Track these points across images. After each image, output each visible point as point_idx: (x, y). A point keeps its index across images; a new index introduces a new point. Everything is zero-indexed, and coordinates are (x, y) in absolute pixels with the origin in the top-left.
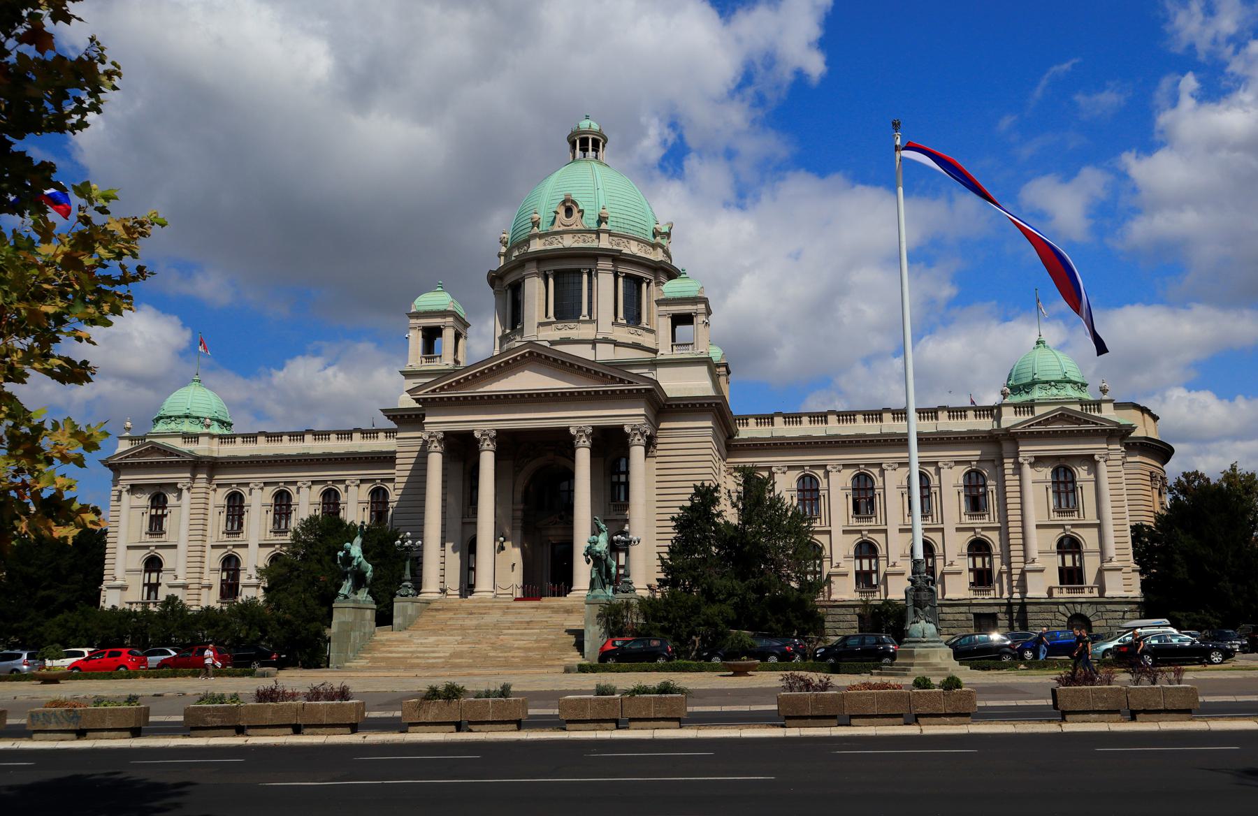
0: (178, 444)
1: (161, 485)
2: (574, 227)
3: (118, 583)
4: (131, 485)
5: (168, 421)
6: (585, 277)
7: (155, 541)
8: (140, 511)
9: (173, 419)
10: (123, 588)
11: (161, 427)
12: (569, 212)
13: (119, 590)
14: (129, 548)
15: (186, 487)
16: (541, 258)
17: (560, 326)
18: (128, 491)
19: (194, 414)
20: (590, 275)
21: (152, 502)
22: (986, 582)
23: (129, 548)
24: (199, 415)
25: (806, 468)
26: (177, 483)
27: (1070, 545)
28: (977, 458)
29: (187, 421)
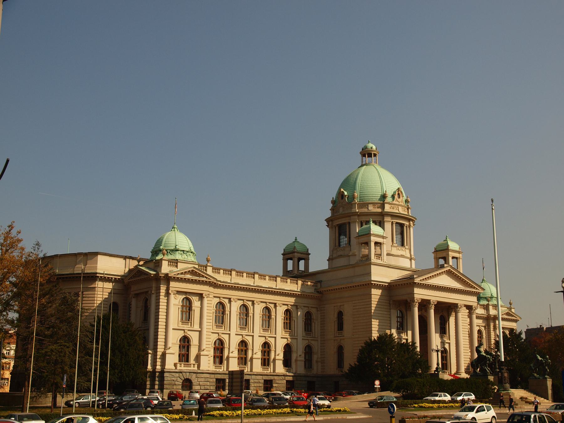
2: (401, 203)
4: (177, 291)
5: (182, 252)
6: (405, 227)
7: (186, 327)
9: (185, 252)
12: (399, 194)
14: (173, 329)
16: (393, 216)
17: (400, 248)
20: (406, 226)
22: (267, 364)
23: (173, 329)
25: (289, 305)
26: (202, 294)
27: (185, 342)
28: (292, 304)
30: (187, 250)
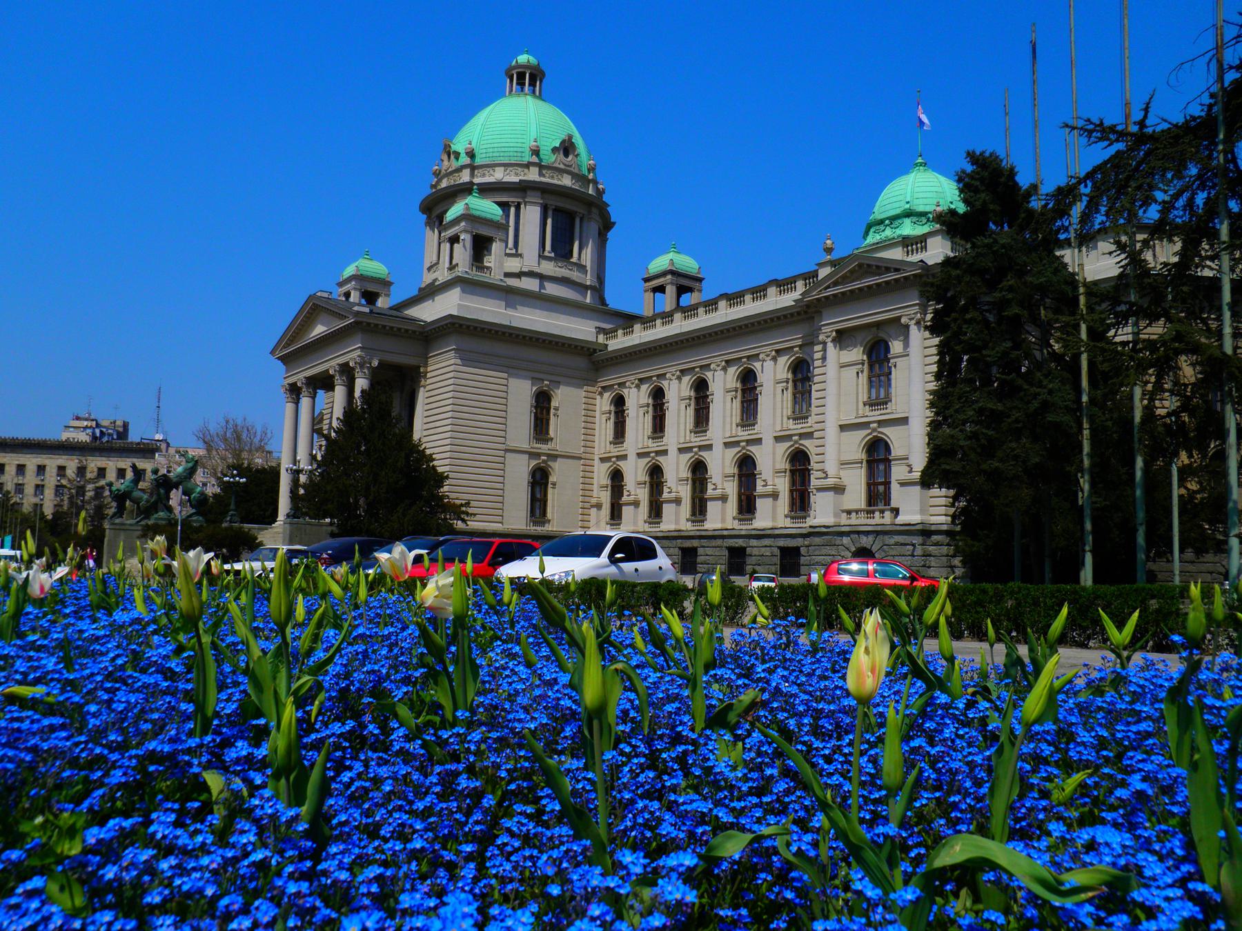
0: (896, 254)
1: (878, 325)
3: (830, 481)
4: (838, 331)
7: (875, 415)
8: (854, 369)
10: (839, 489)
11: (872, 238)
13: (831, 494)
14: (843, 428)
15: (913, 322)
18: (833, 341)
19: (921, 209)
21: (869, 357)
23: (843, 428)
24: (928, 209)
26: (899, 318)
29: (907, 221)
30: (898, 211)
